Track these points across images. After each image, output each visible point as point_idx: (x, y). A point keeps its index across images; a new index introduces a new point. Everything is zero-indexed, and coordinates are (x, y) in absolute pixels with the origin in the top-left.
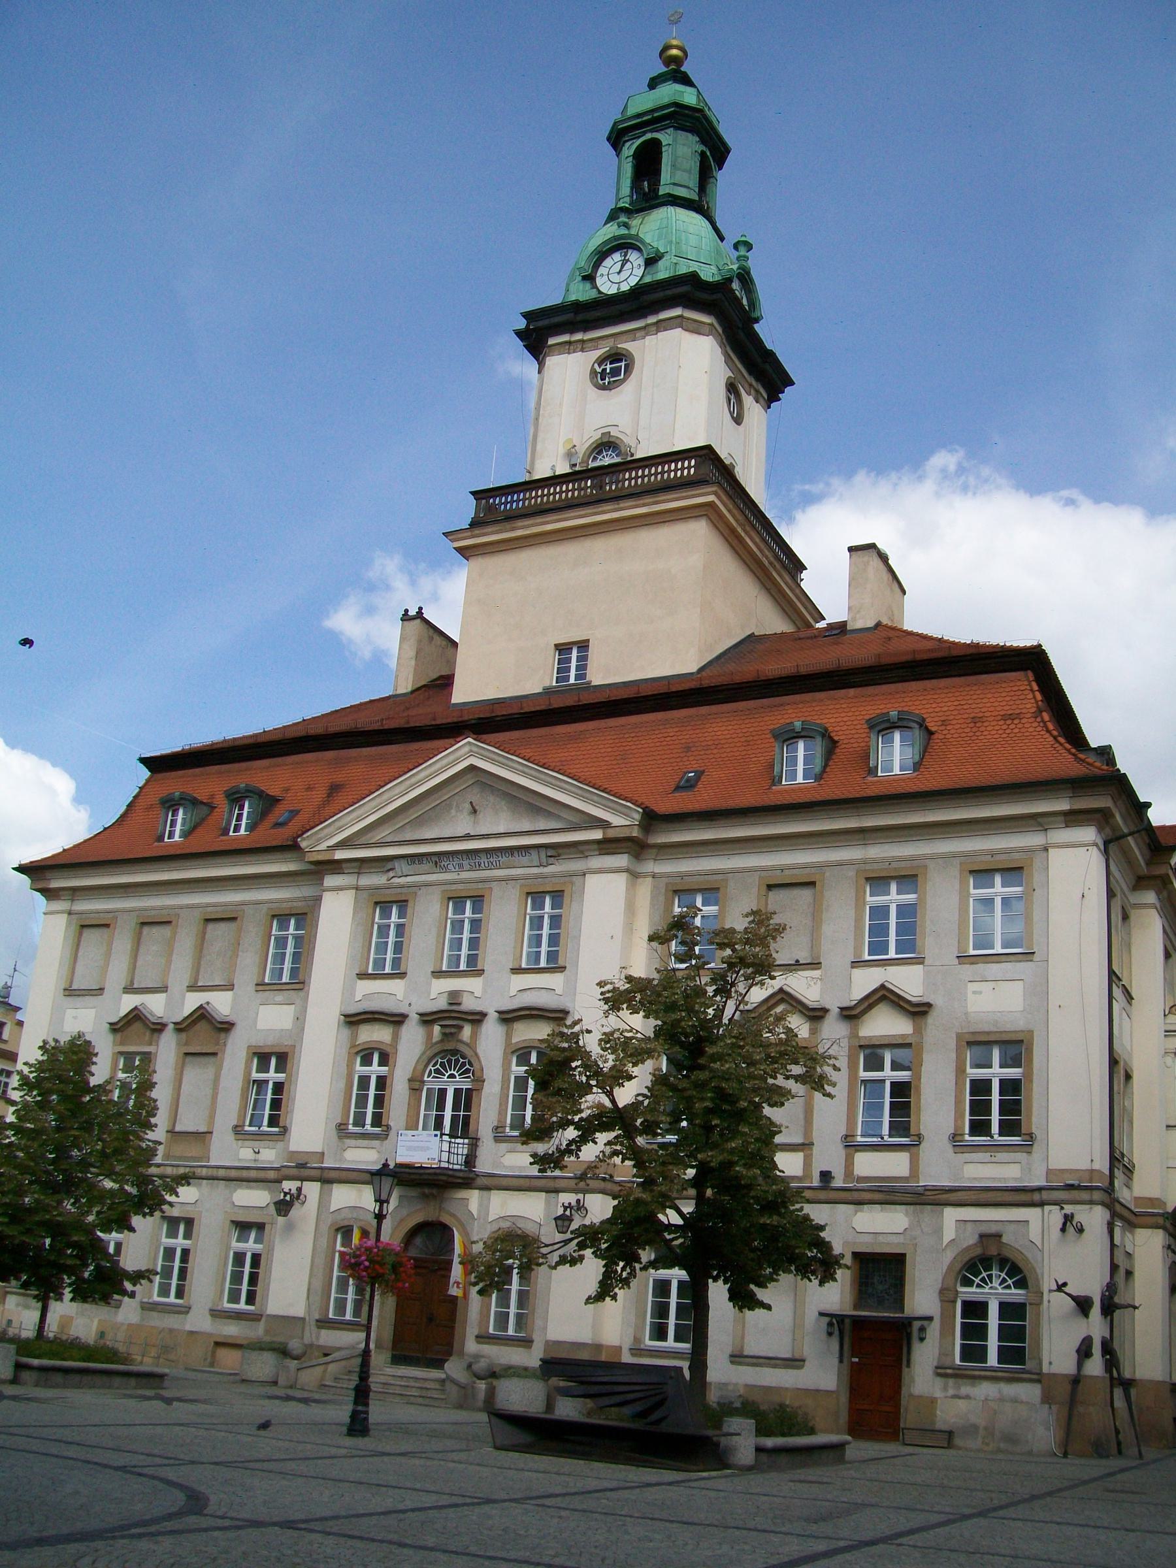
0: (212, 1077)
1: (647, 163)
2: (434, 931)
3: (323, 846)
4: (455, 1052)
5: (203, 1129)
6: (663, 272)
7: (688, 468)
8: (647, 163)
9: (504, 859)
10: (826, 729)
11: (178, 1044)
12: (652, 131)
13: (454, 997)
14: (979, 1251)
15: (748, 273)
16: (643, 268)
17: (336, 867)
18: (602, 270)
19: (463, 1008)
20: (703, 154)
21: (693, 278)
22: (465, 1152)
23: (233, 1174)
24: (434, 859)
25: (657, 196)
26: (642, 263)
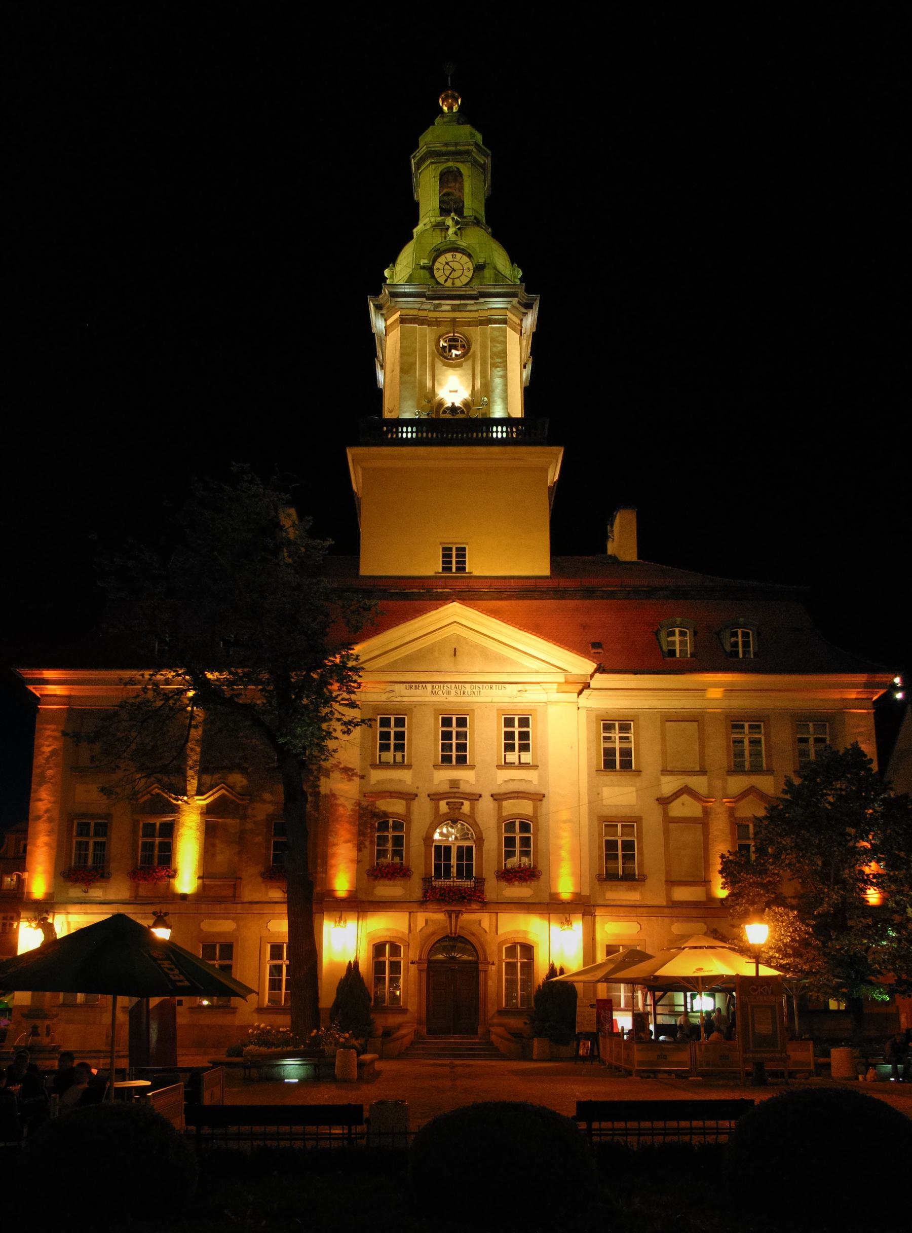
16: (472, 272)
18: (437, 265)
19: (460, 790)
26: (471, 268)
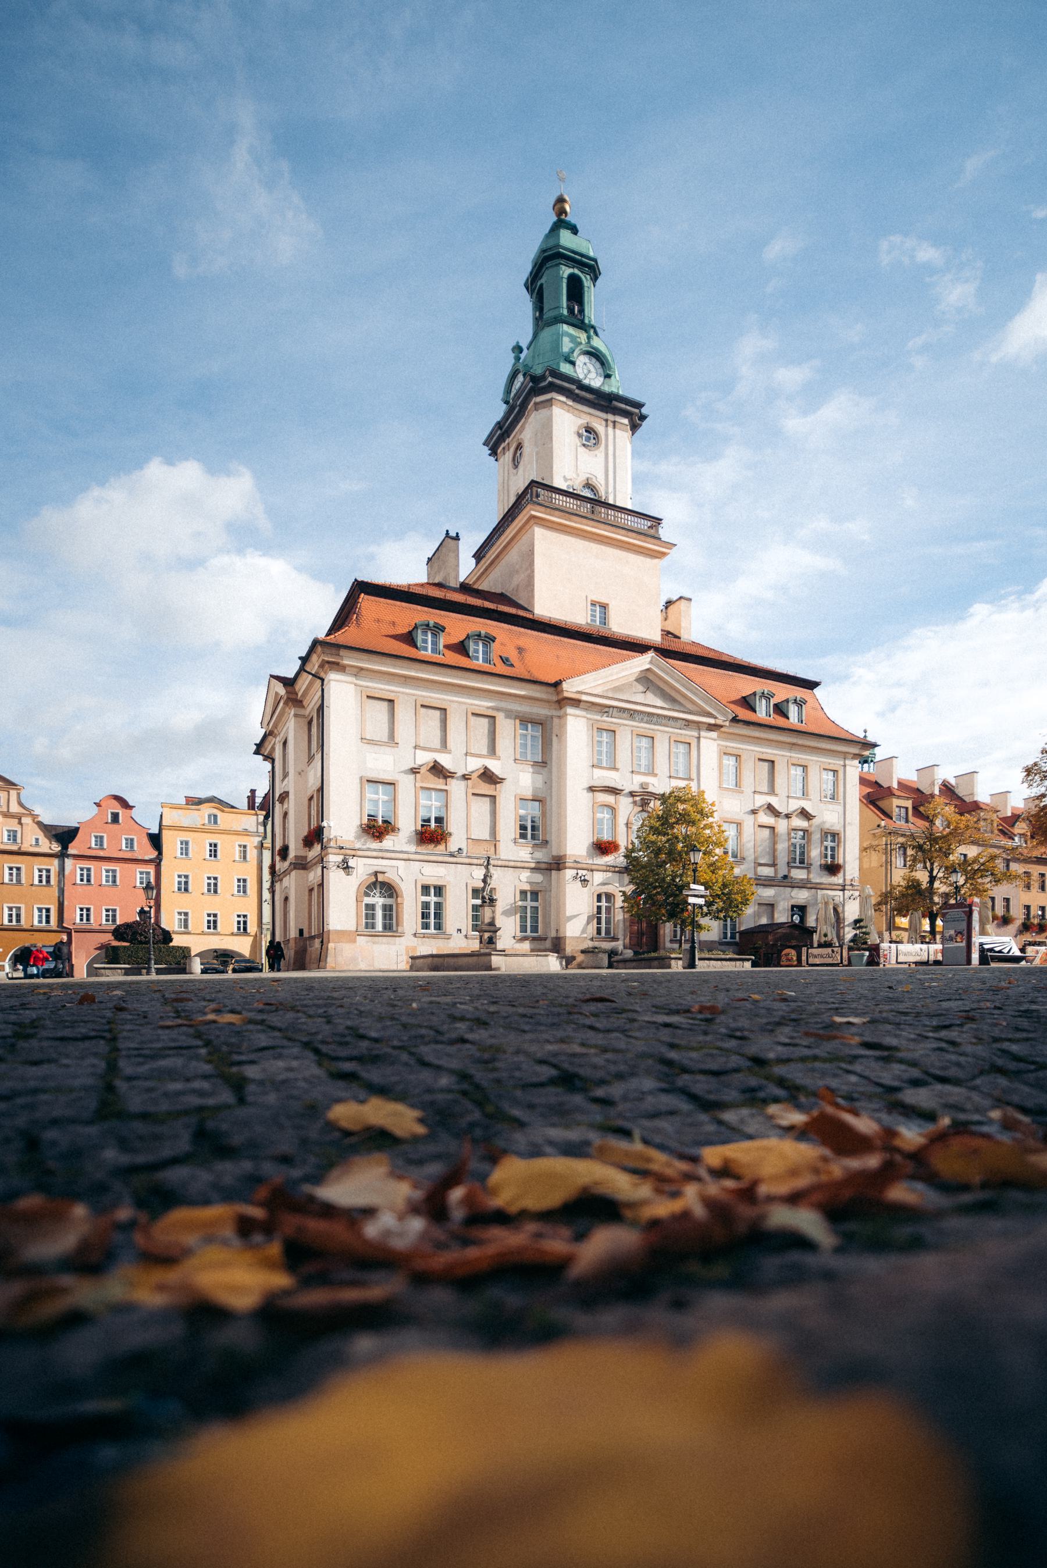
17: (576, 703)
23: (519, 864)
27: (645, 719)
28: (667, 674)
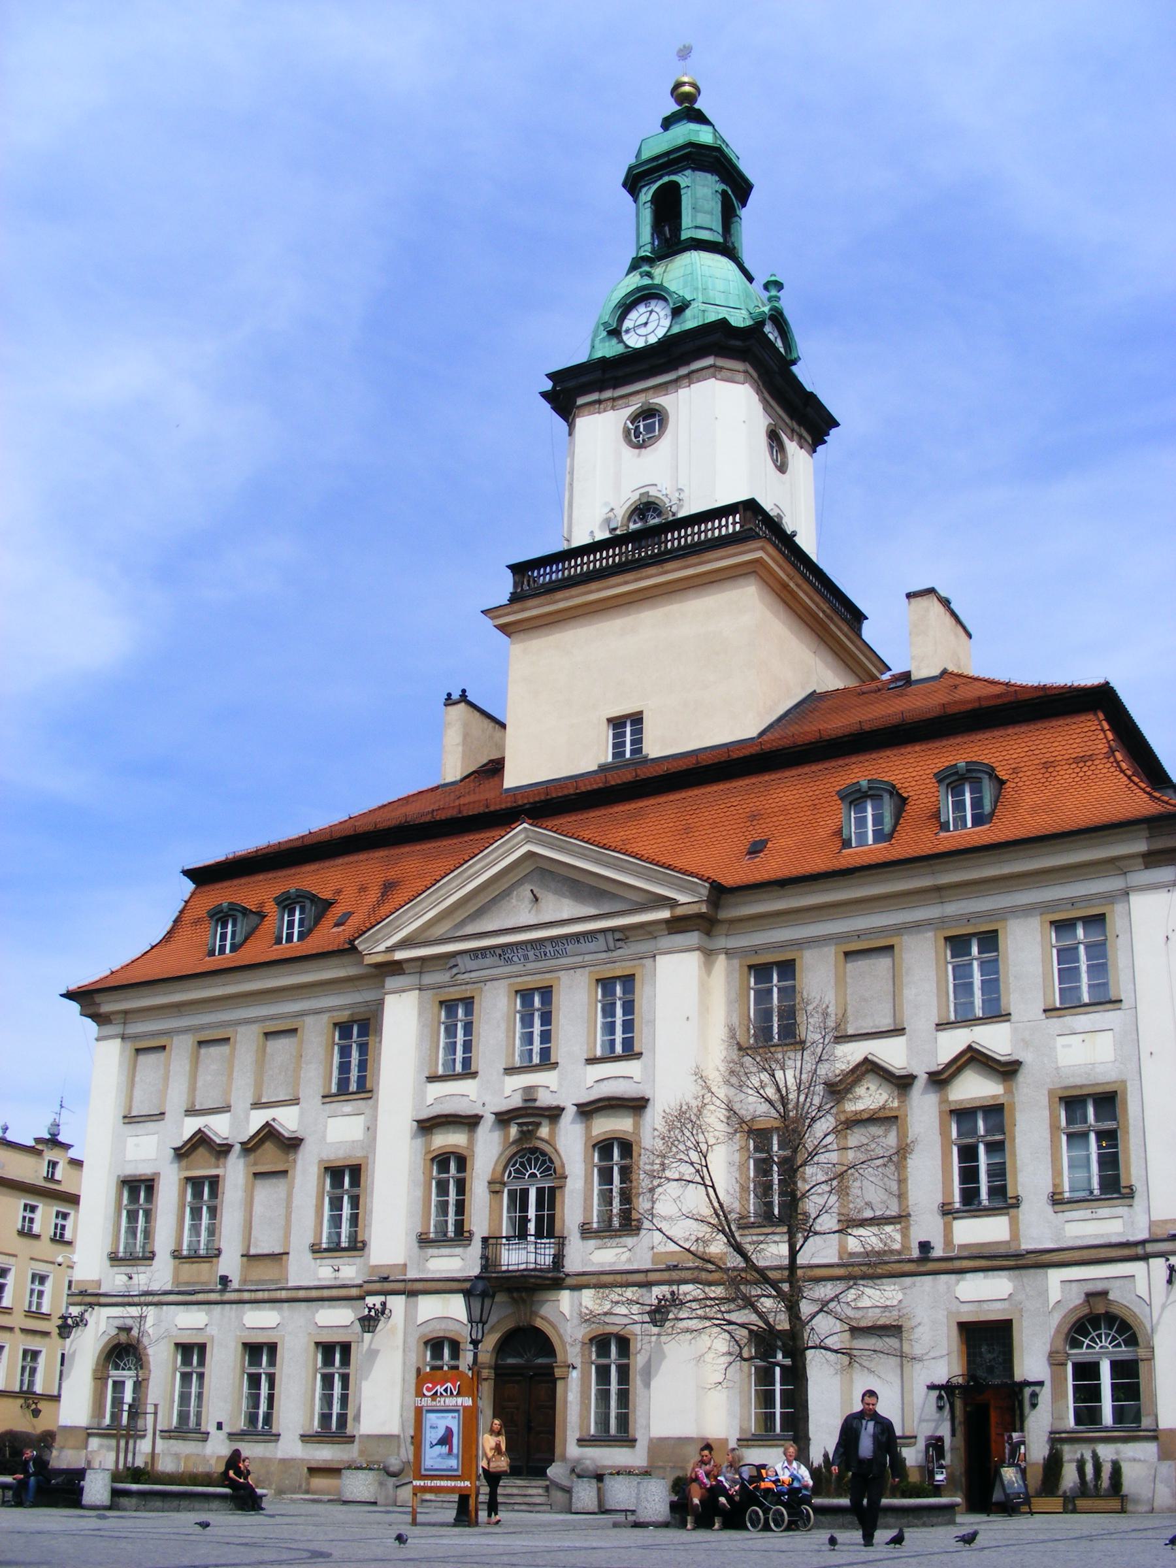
0: (283, 1195)
1: (667, 208)
2: (503, 1026)
3: (382, 948)
4: (534, 1150)
5: (277, 1250)
6: (690, 321)
7: (731, 525)
8: (667, 208)
9: (570, 948)
10: (894, 787)
11: (247, 1165)
12: (669, 174)
13: (529, 1093)
14: (1086, 1310)
15: (781, 314)
17: (396, 968)
18: (627, 324)
19: (538, 1104)
20: (724, 193)
21: (723, 323)
22: (552, 1251)
23: (314, 1294)
24: (499, 951)
25: (679, 242)
26: (669, 313)
27: (531, 954)
28: (561, 849)
